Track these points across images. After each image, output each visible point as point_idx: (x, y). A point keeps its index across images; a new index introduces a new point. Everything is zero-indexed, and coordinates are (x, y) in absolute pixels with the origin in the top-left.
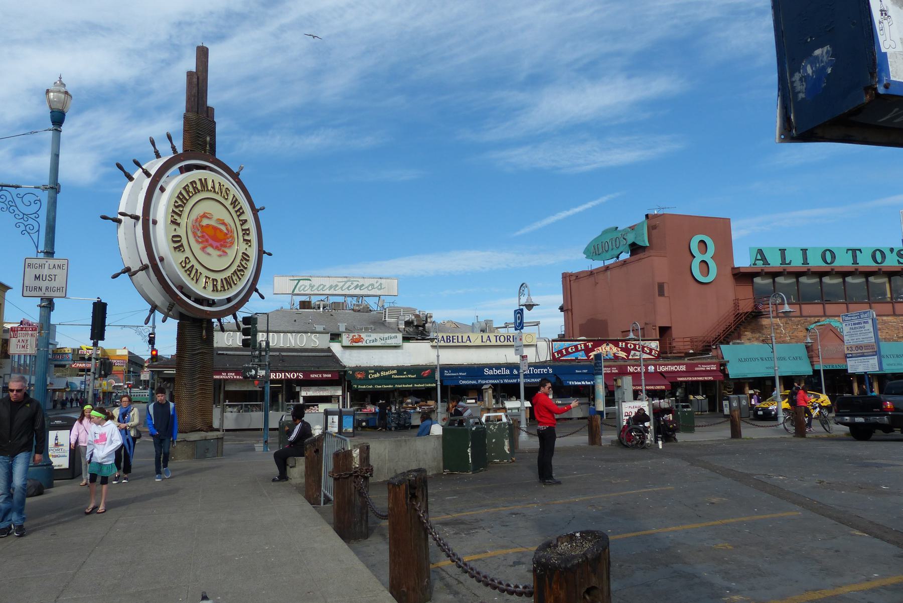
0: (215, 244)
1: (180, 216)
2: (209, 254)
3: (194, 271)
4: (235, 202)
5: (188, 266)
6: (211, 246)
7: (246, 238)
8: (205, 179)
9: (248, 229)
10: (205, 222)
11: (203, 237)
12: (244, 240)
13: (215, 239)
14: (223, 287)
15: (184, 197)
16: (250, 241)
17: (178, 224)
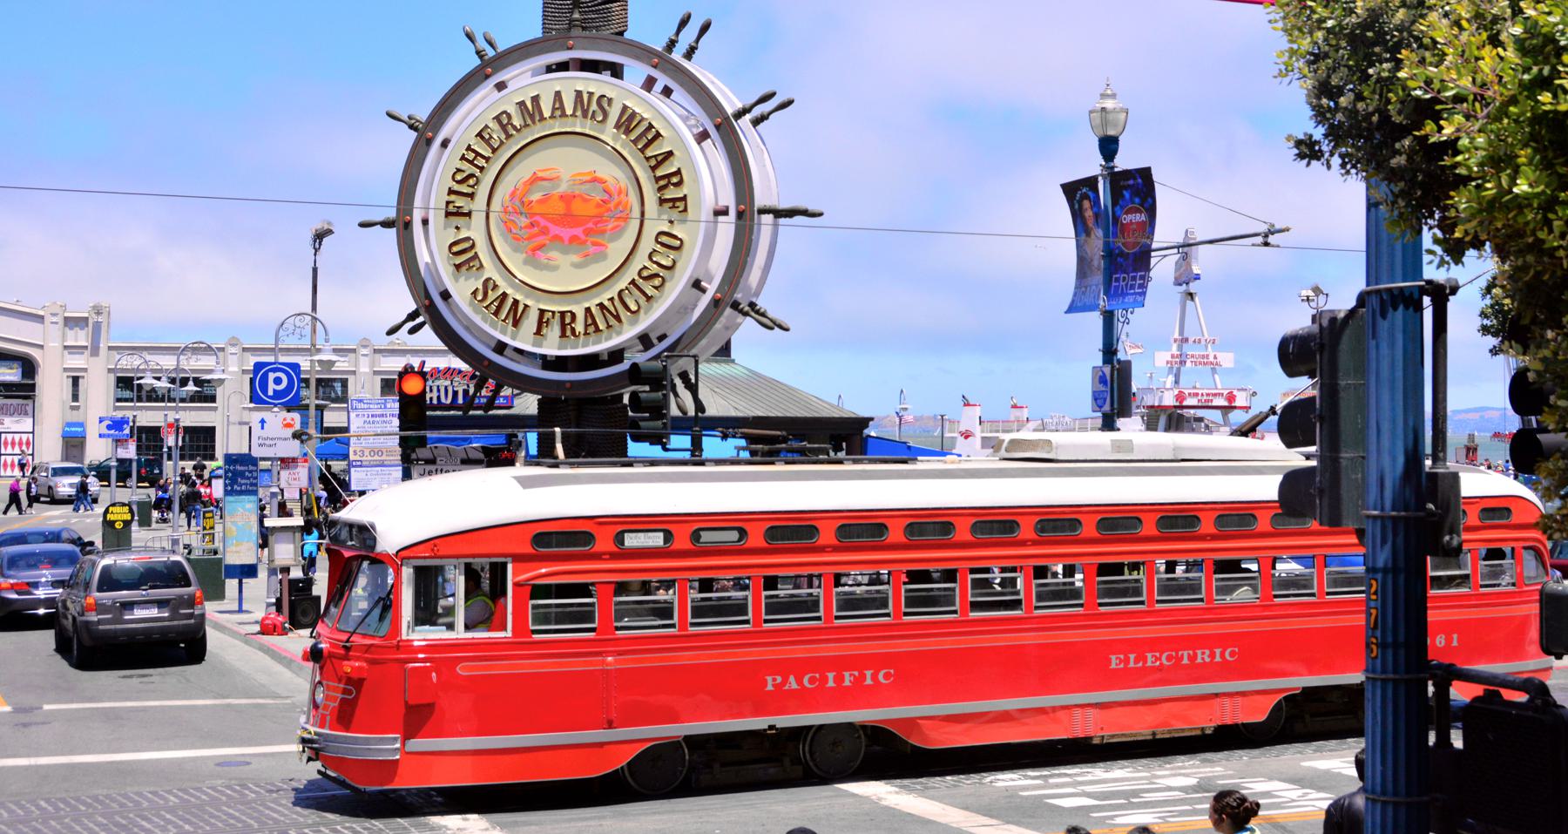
0: (566, 233)
1: (471, 196)
3: (509, 302)
4: (628, 122)
5: (492, 296)
6: (556, 238)
7: (670, 193)
8: (535, 99)
9: (678, 172)
11: (532, 225)
12: (662, 201)
13: (568, 219)
16: (684, 198)
17: (469, 214)
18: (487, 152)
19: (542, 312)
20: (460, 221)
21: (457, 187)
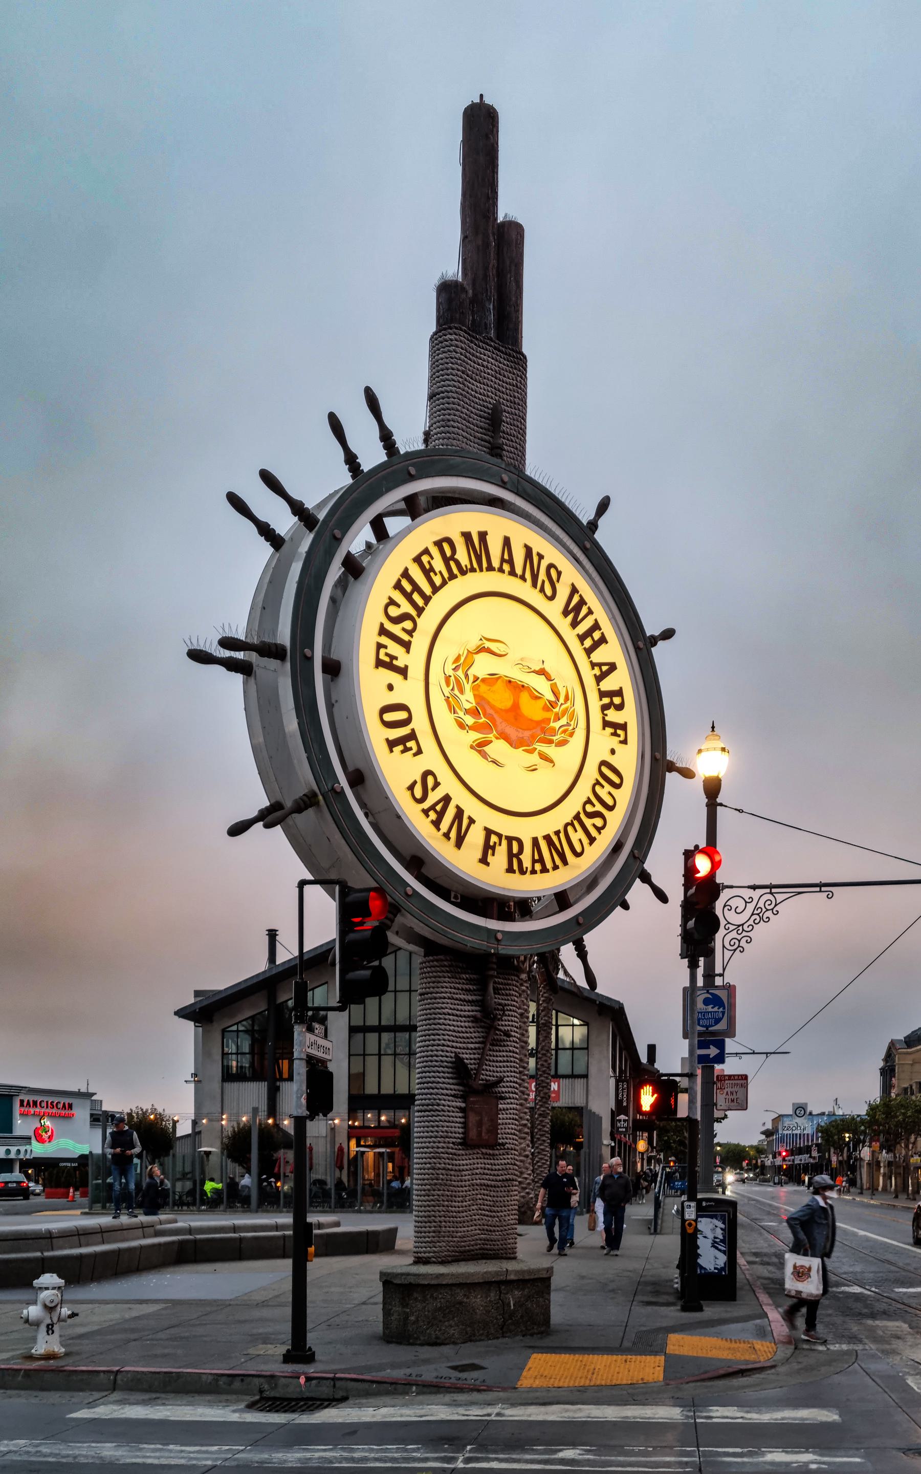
1: (407, 646)
2: (494, 762)
5: (434, 797)
10: (483, 666)
14: (541, 860)
15: (416, 588)
18: (428, 590)
19: (489, 832)
20: (395, 678)
21: (389, 626)
